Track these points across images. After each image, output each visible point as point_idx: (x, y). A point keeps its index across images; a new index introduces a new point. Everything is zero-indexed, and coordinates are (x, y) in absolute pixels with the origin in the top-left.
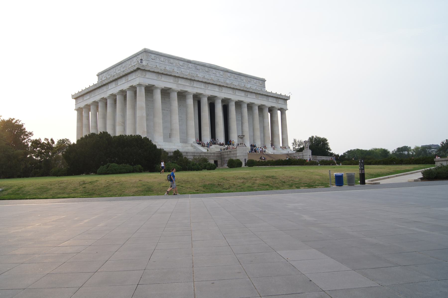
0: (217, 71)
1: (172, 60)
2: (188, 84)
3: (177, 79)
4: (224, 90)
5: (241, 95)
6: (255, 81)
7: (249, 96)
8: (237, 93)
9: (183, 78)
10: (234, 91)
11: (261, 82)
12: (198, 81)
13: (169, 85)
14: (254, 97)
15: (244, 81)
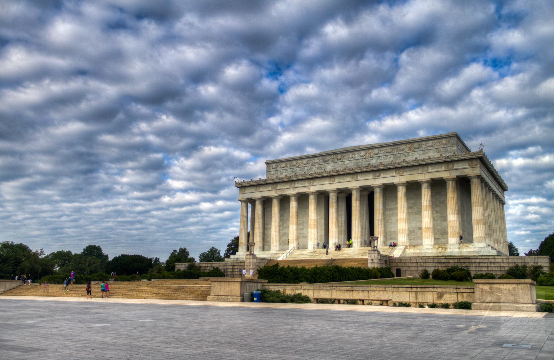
0: (357, 153)
1: (294, 163)
2: (288, 187)
3: (275, 186)
4: (337, 180)
5: (368, 178)
6: (430, 143)
7: (382, 175)
8: (360, 177)
9: (279, 182)
10: (355, 176)
11: (444, 141)
12: (298, 180)
13: (266, 194)
14: (394, 174)
15: (406, 150)
